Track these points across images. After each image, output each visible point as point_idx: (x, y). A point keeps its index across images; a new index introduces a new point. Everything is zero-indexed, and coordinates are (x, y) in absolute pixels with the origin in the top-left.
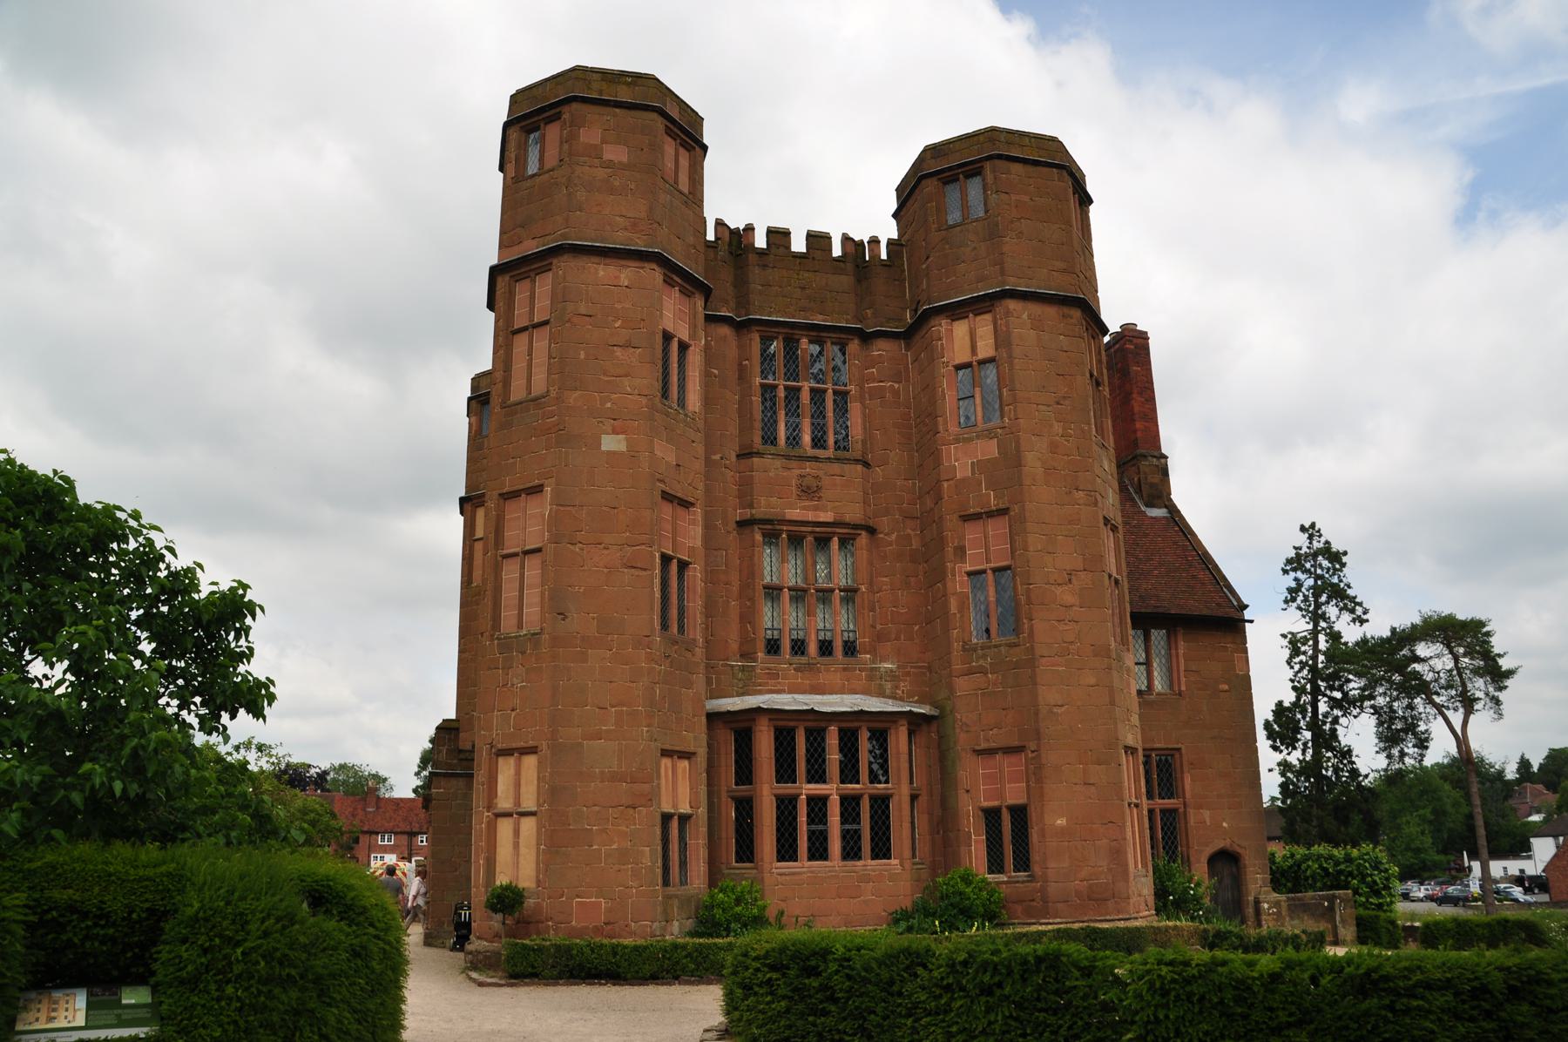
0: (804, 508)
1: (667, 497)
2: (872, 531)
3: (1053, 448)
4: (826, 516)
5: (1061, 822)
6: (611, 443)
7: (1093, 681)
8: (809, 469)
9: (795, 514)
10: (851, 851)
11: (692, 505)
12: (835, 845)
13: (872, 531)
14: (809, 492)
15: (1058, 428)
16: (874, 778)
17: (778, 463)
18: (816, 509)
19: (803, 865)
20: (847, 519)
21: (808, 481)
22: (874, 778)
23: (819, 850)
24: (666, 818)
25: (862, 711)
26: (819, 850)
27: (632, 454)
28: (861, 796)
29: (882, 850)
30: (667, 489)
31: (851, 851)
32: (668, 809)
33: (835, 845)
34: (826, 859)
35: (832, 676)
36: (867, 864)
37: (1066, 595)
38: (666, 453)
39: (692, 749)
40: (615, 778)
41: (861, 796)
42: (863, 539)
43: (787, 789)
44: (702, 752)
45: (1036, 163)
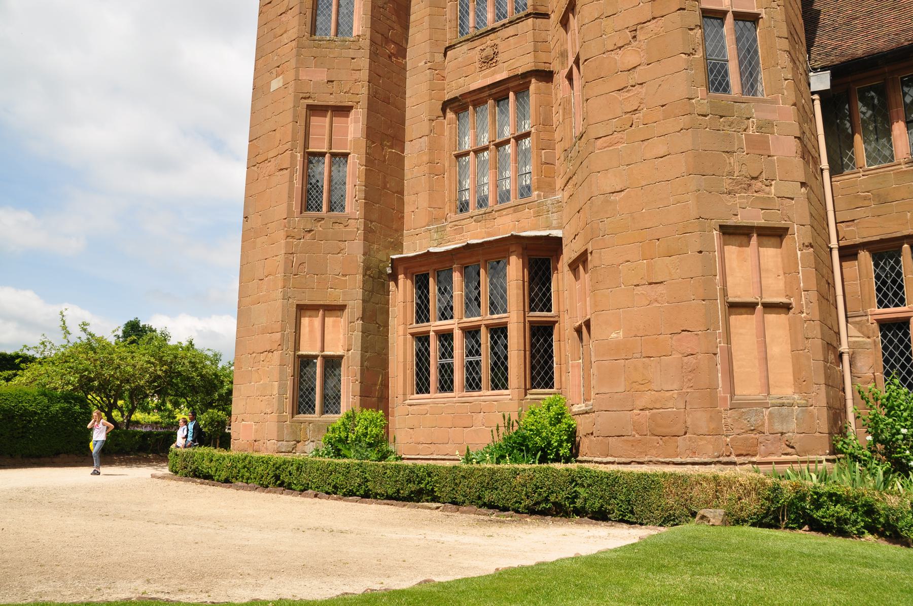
0: (485, 77)
1: (315, 110)
2: (546, 76)
5: (616, 335)
8: (489, 40)
10: (473, 384)
11: (351, 108)
12: (459, 376)
13: (546, 76)
16: (493, 308)
17: (465, 47)
18: (494, 73)
19: (434, 396)
21: (489, 52)
22: (493, 308)
23: (446, 385)
24: (305, 362)
25: (468, 246)
26: (446, 385)
27: (286, 85)
28: (480, 326)
29: (500, 381)
30: (316, 103)
31: (473, 384)
32: (305, 351)
33: (459, 376)
34: (452, 390)
36: (486, 393)
37: (629, 57)
39: (340, 302)
41: (480, 326)
42: (534, 85)
43: (422, 327)
44: (355, 306)
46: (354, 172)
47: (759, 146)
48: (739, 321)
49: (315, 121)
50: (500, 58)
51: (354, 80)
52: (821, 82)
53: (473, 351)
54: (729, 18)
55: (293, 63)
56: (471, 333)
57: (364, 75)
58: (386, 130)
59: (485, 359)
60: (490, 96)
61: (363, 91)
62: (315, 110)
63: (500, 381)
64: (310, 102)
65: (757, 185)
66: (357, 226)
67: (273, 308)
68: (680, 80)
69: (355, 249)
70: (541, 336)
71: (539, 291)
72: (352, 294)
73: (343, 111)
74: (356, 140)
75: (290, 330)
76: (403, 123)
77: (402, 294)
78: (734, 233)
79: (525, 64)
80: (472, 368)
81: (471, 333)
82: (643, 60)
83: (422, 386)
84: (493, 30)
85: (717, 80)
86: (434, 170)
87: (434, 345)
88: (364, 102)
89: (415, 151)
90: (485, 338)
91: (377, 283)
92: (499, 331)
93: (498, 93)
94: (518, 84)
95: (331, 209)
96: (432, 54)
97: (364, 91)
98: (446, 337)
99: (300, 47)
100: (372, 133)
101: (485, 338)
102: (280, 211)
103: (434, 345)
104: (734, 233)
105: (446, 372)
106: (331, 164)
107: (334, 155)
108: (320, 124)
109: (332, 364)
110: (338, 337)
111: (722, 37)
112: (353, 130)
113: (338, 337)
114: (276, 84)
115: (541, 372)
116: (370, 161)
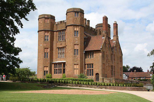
6: (41, 45)
8: (61, 42)
9: (60, 47)
12: (58, 73)
14: (61, 44)
17: (59, 42)
19: (56, 74)
20: (64, 46)
23: (57, 73)
24: (45, 71)
26: (57, 73)
29: (61, 73)
31: (59, 73)
35: (62, 59)
37: (70, 52)
40: (41, 68)
44: (49, 66)
45: (70, 12)
46: (49, 54)
47: (77, 59)
48: (75, 70)
49: (45, 49)
52: (84, 52)
53: (59, 71)
56: (59, 69)
57: (50, 45)
59: (60, 71)
63: (61, 73)
66: (49, 59)
67: (42, 66)
68: (72, 54)
69: (49, 61)
70: (64, 70)
71: (64, 66)
72: (49, 65)
75: (43, 69)
77: (53, 66)
78: (75, 64)
79: (64, 46)
80: (59, 72)
81: (59, 69)
83: (55, 73)
85: (75, 54)
86: (56, 54)
87: (56, 70)
89: (54, 52)
90: (60, 70)
91: (51, 64)
92: (61, 69)
93: (62, 48)
94: (64, 47)
98: (57, 69)
100: (50, 51)
101: (60, 70)
102: (42, 58)
103: (56, 70)
104: (75, 64)
105: (57, 72)
108: (46, 50)
109: (47, 71)
110: (47, 69)
112: (49, 50)
113: (47, 69)
115: (64, 72)
116: (50, 53)
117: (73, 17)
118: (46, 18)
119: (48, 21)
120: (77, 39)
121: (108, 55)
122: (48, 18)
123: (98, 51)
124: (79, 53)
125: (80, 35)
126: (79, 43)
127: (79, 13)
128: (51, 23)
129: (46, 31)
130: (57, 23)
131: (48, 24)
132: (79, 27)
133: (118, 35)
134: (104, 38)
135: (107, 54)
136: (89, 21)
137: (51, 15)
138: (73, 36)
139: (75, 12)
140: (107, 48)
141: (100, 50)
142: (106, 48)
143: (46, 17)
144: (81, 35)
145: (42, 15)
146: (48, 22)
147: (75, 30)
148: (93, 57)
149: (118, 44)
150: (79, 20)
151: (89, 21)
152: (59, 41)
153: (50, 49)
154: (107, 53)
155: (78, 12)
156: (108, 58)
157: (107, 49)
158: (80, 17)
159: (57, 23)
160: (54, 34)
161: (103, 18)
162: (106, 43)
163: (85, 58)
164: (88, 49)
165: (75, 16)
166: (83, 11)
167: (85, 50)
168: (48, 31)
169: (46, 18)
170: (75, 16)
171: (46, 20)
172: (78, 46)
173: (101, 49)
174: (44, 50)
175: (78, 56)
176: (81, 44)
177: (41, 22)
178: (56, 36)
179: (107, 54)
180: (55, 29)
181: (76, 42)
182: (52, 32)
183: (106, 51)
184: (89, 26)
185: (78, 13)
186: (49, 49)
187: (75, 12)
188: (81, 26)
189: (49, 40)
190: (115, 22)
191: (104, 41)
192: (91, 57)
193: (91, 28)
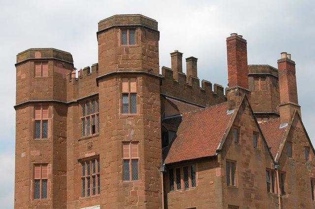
3: (107, 124)
4: (93, 154)
7: (113, 195)
8: (90, 140)
9: (87, 155)
11: (48, 164)
14: (90, 148)
15: (108, 118)
17: (84, 141)
21: (90, 145)
30: (36, 163)
37: (108, 170)
38: (36, 153)
45: (107, 30)
47: (134, 193)
50: (93, 147)
51: (50, 155)
52: (163, 169)
54: (130, 161)
55: (28, 148)
57: (52, 152)
58: (60, 168)
60: (90, 160)
61: (51, 158)
62: (37, 165)
64: (34, 162)
65: (133, 203)
73: (45, 165)
74: (50, 175)
76: (66, 165)
82: (110, 172)
84: (91, 137)
85: (125, 177)
88: (52, 162)
95: (42, 198)
96: (75, 141)
97: (52, 157)
99: (30, 143)
100: (55, 171)
106: (42, 182)
107: (43, 180)
108: (38, 169)
111: (128, 166)
112: (49, 169)
114: (23, 155)
116: (54, 181)
117: (116, 45)
118: (37, 62)
119: (45, 70)
120: (130, 123)
121: (253, 172)
122: (43, 61)
123: (208, 161)
124: (142, 173)
125: (144, 107)
126: (141, 138)
127: (139, 31)
128: (57, 76)
129: (37, 105)
130: (77, 77)
131: (45, 79)
132: (140, 79)
133: (297, 102)
134: (233, 112)
135: (249, 172)
136: (193, 61)
137: (54, 50)
138: (117, 113)
139: (124, 29)
140: (248, 149)
141: (215, 158)
142: (244, 148)
143: (38, 56)
144: (147, 106)
145: (26, 51)
146: (46, 74)
147: (125, 90)
148: (193, 185)
149: (302, 134)
150: (138, 56)
151: (193, 61)
152: (84, 137)
153: (54, 166)
154: (251, 167)
155: (132, 28)
156: (252, 184)
157: (247, 153)
158: (140, 43)
159: (77, 77)
160: (65, 114)
161: (229, 40)
162: (243, 128)
163: (168, 187)
164: (176, 155)
165: (122, 44)
166: (155, 23)
167: (168, 161)
168: (45, 104)
169: (37, 62)
170: (122, 44)
171: (38, 67)
172: (136, 147)
173: (218, 151)
174: (32, 170)
175: (138, 185)
176: (148, 139)
177: (23, 76)
178: (75, 122)
179: (249, 172)
180: (72, 95)
181: (131, 135)
182: (61, 107)
183: (244, 160)
184: (195, 80)
185: (135, 29)
186: (50, 165)
187: (124, 29)
188: (145, 77)
189: (50, 134)
190: (284, 56)
191: (230, 124)
192: (187, 186)
193: (208, 84)
